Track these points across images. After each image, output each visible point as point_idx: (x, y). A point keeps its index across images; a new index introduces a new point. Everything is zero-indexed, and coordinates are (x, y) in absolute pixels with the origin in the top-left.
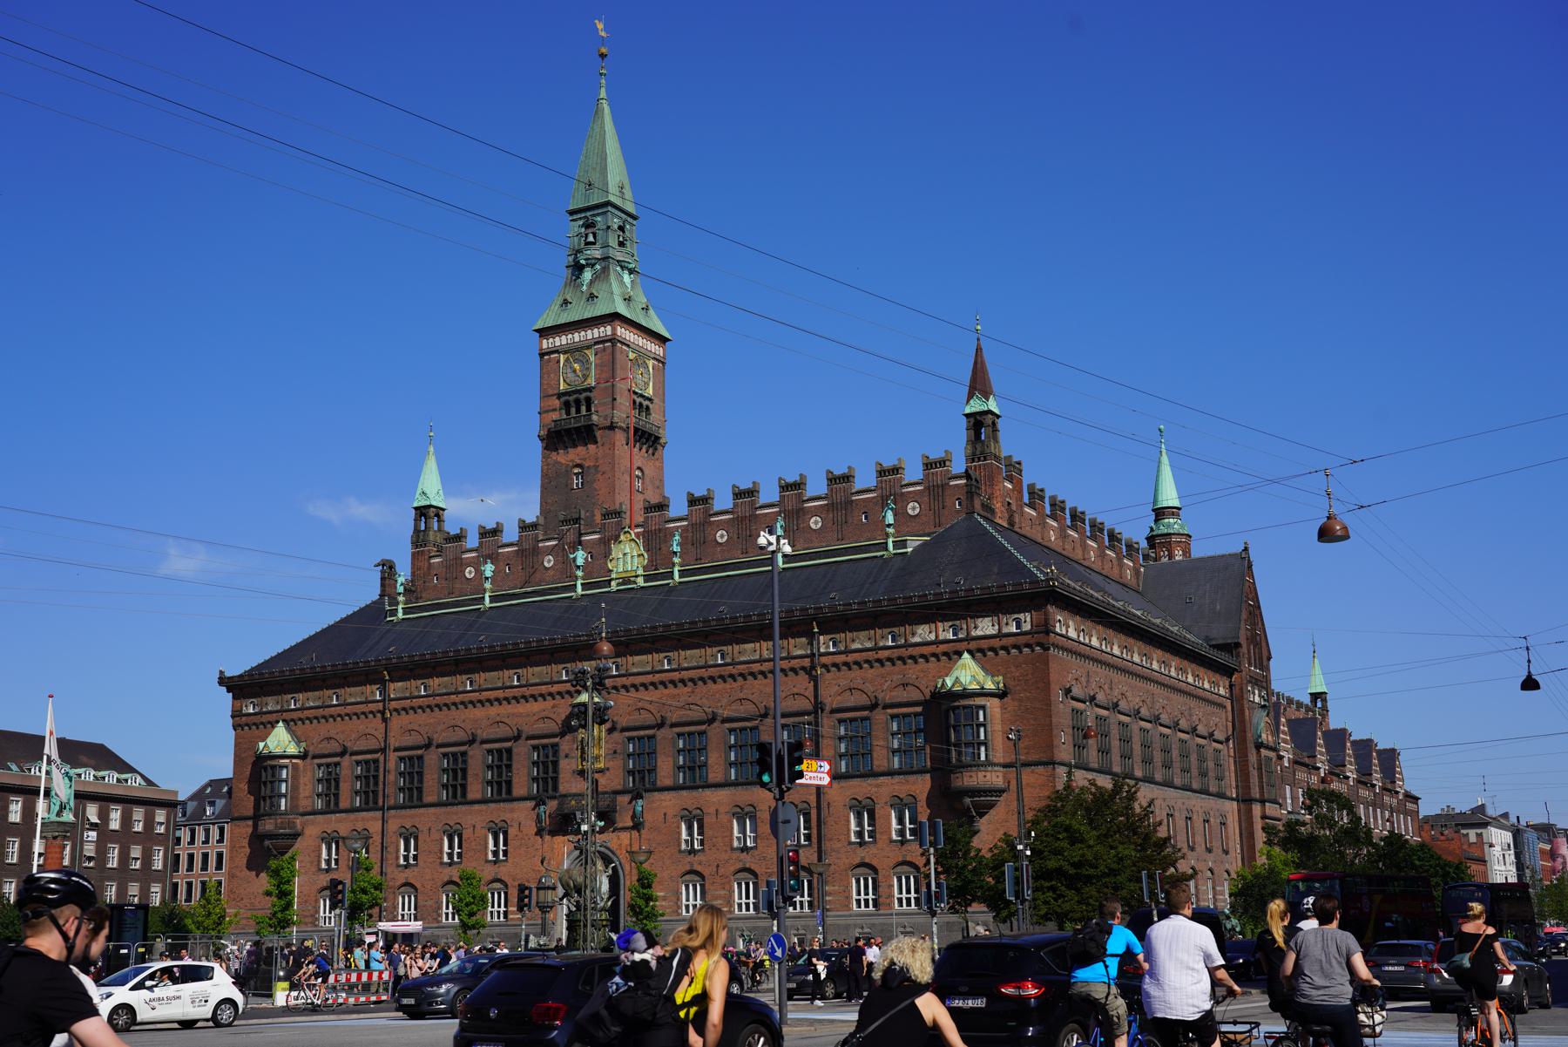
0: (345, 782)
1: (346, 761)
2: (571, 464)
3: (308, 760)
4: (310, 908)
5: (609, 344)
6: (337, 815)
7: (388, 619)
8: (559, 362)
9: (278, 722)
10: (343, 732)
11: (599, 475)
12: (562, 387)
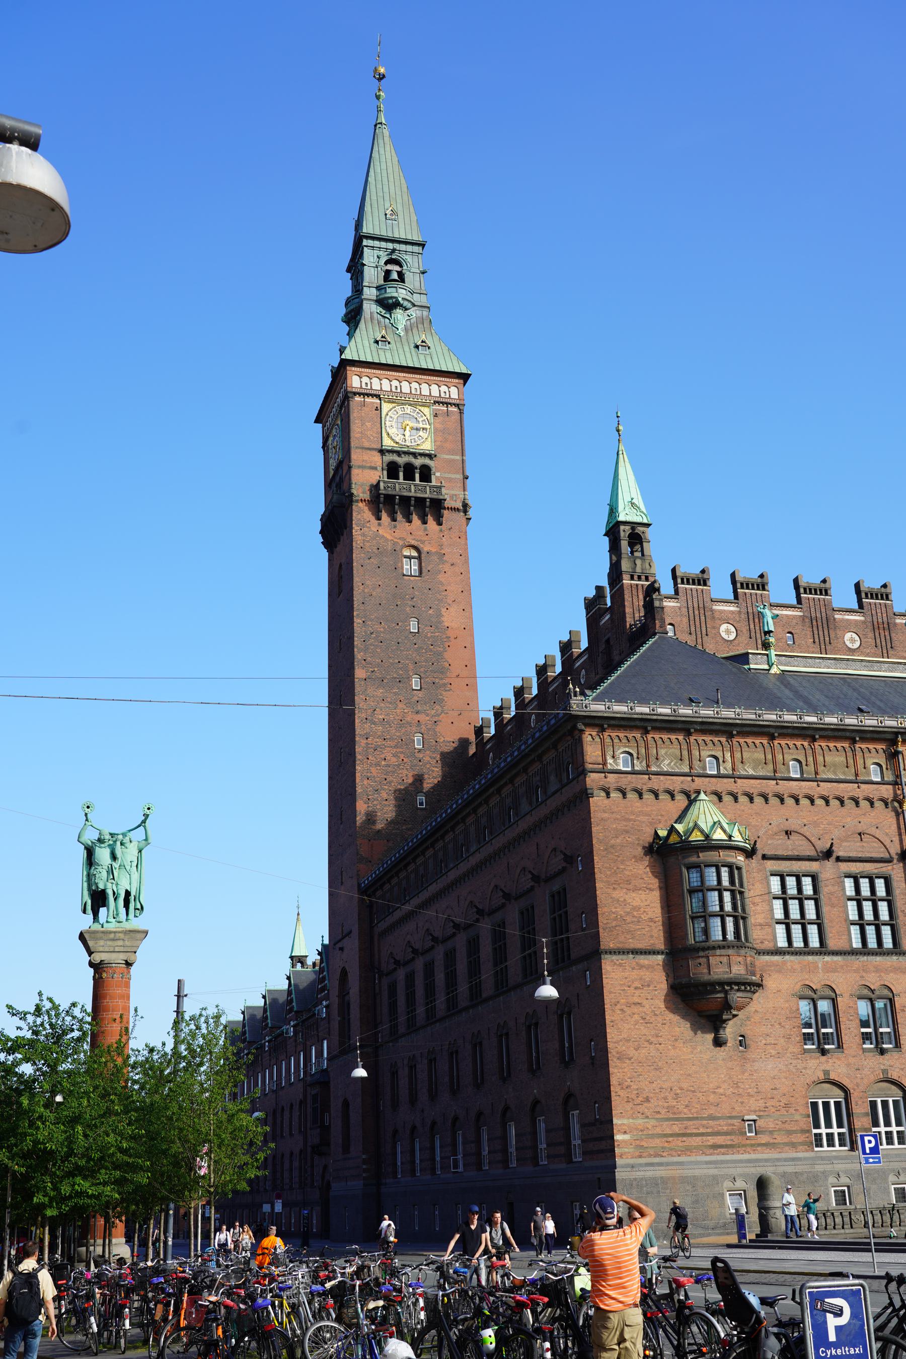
0: (833, 906)
1: (827, 870)
2: (401, 543)
3: (755, 861)
4: (797, 1117)
5: (455, 409)
6: (827, 958)
7: (752, 666)
8: (379, 409)
9: (698, 792)
10: (816, 824)
11: (447, 567)
12: (387, 443)
